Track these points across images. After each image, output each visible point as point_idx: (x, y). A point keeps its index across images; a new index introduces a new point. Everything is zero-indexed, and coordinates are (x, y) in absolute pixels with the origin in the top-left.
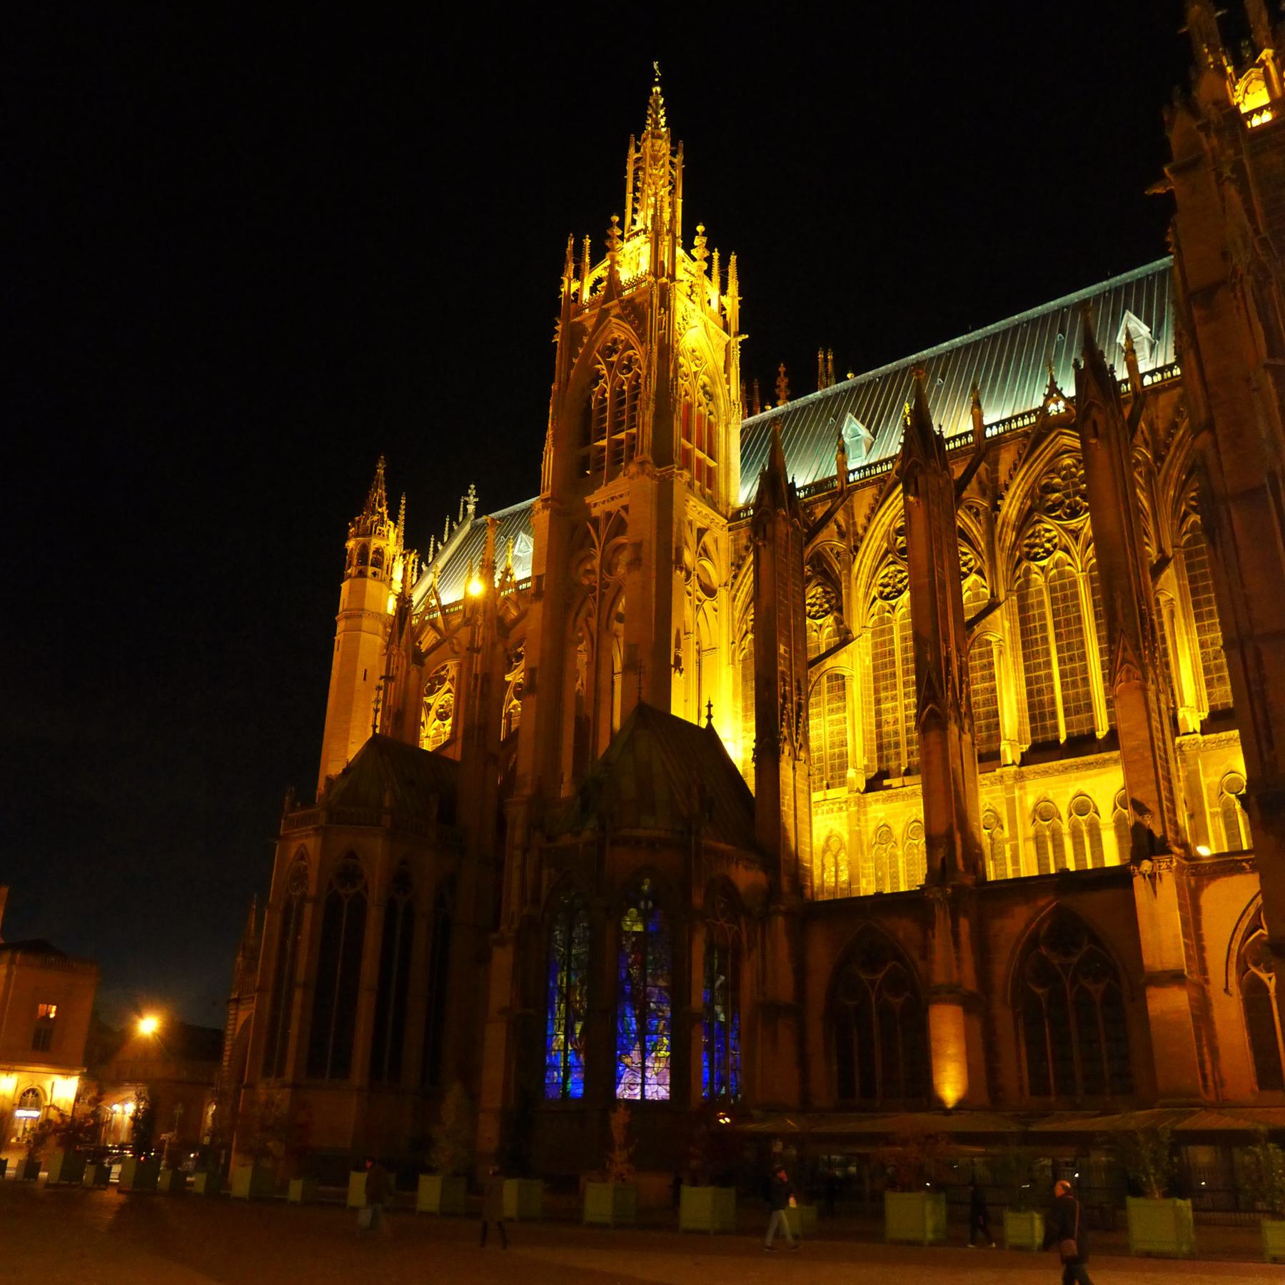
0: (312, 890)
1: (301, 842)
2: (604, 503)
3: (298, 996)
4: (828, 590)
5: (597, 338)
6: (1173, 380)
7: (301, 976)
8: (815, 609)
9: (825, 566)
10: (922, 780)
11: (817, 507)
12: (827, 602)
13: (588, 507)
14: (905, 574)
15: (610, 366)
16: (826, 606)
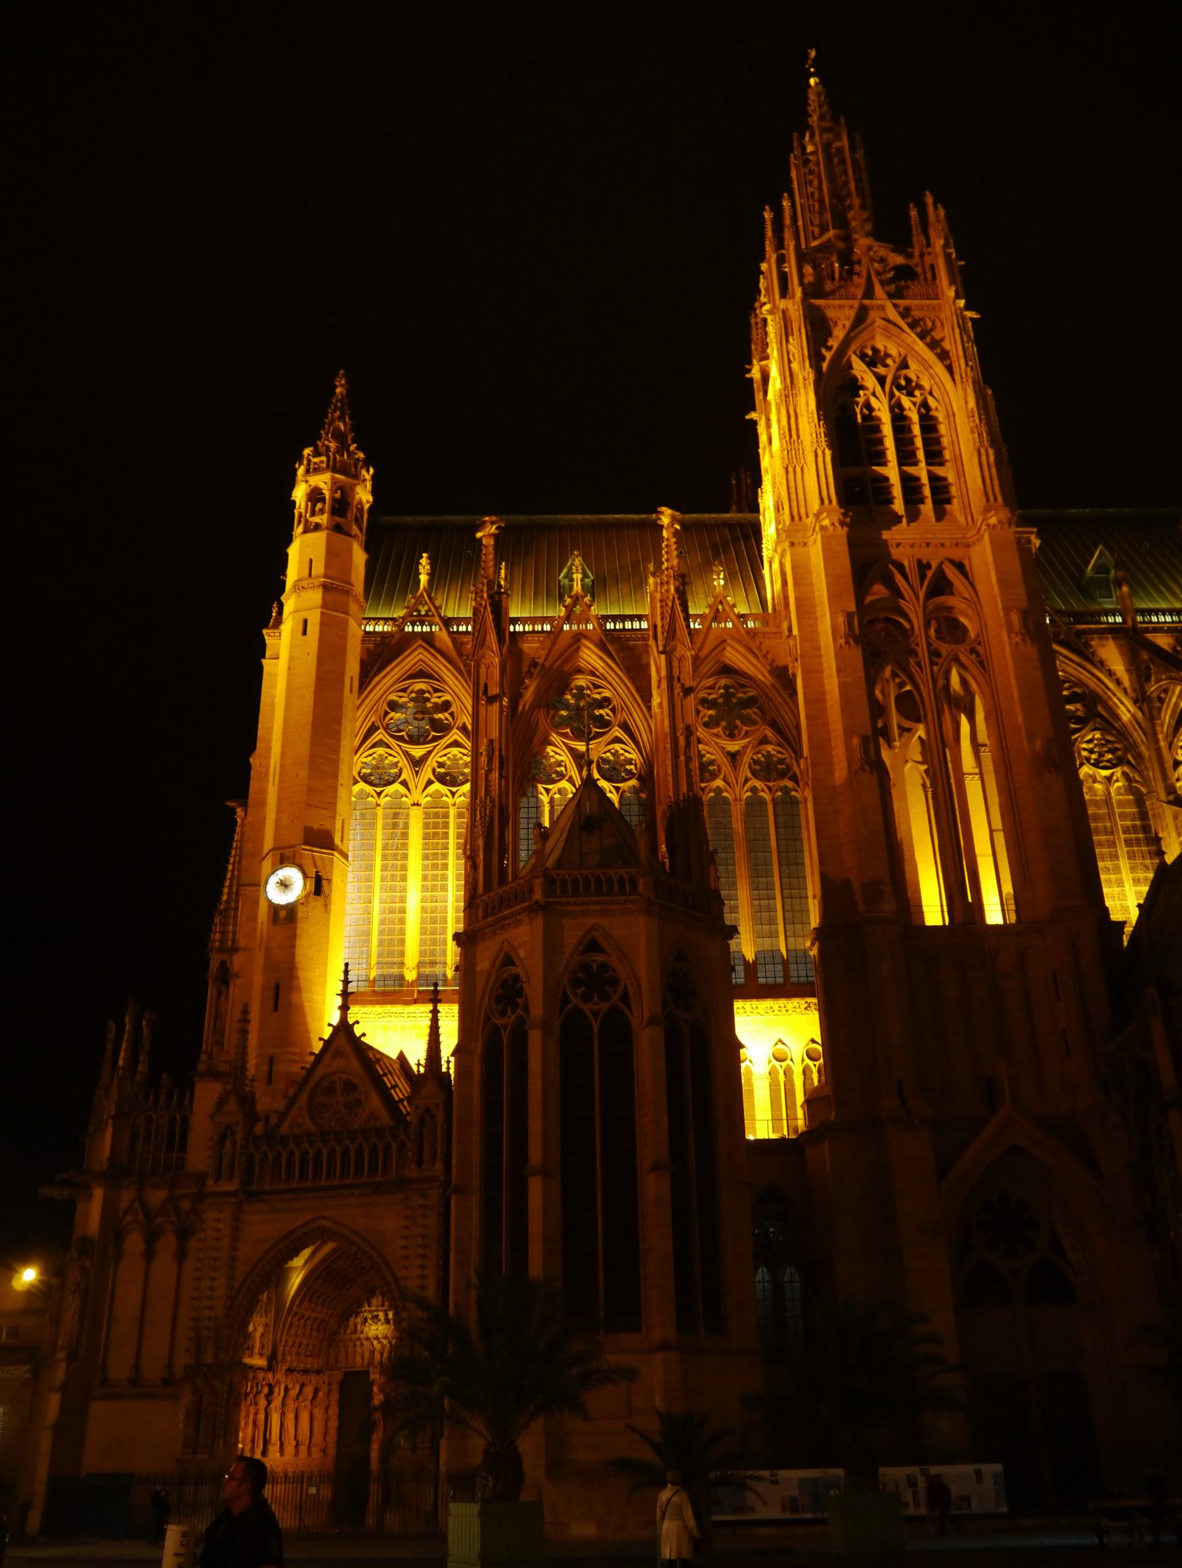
0: (537, 1010)
1: (590, 921)
2: (912, 546)
3: (535, 1186)
4: (1109, 738)
5: (853, 339)
6: (1157, 625)
7: (535, 1154)
8: (1094, 756)
9: (1100, 709)
10: (459, 999)
11: (1093, 639)
12: (1109, 751)
13: (885, 544)
14: (1084, 746)
15: (881, 380)
16: (1110, 756)
